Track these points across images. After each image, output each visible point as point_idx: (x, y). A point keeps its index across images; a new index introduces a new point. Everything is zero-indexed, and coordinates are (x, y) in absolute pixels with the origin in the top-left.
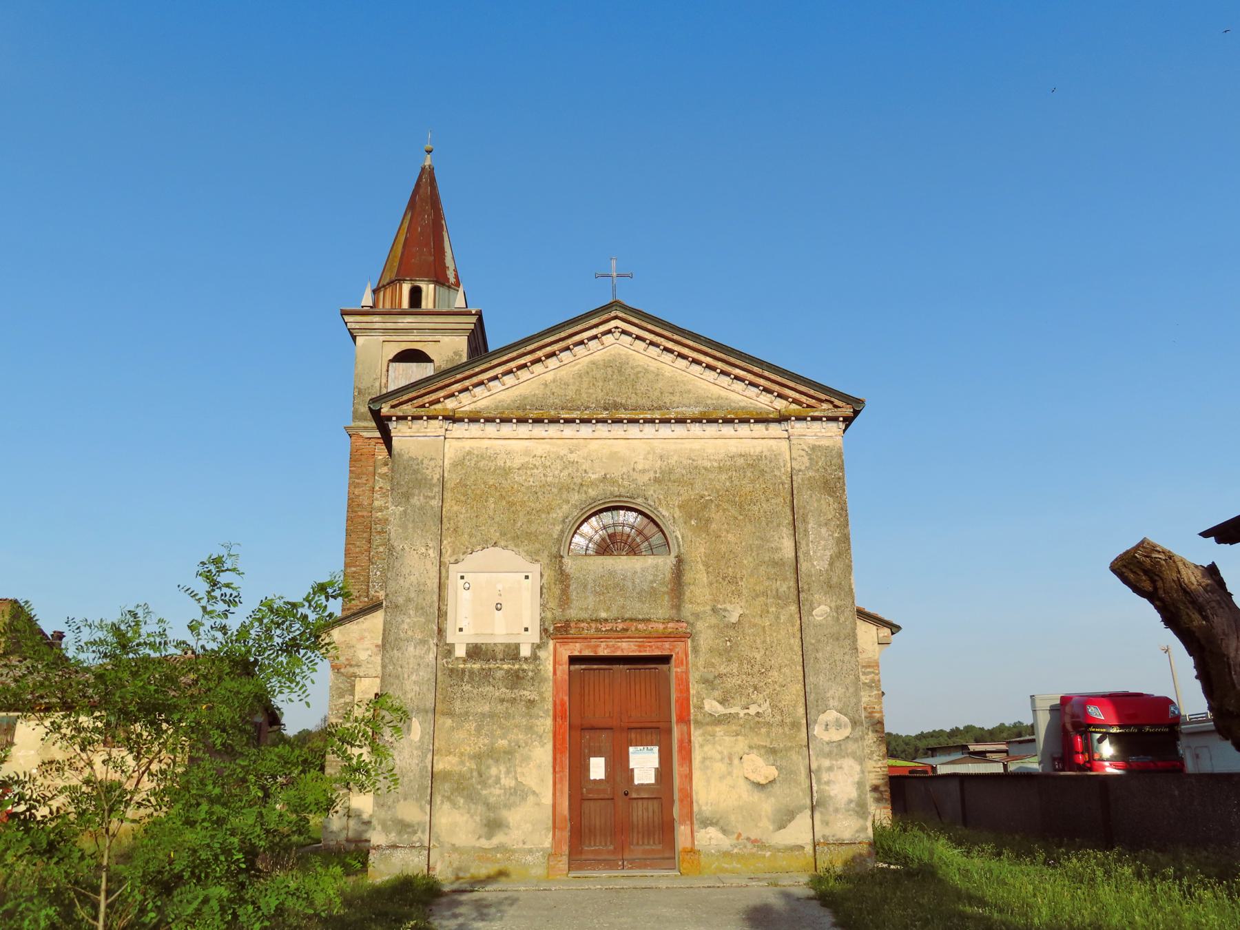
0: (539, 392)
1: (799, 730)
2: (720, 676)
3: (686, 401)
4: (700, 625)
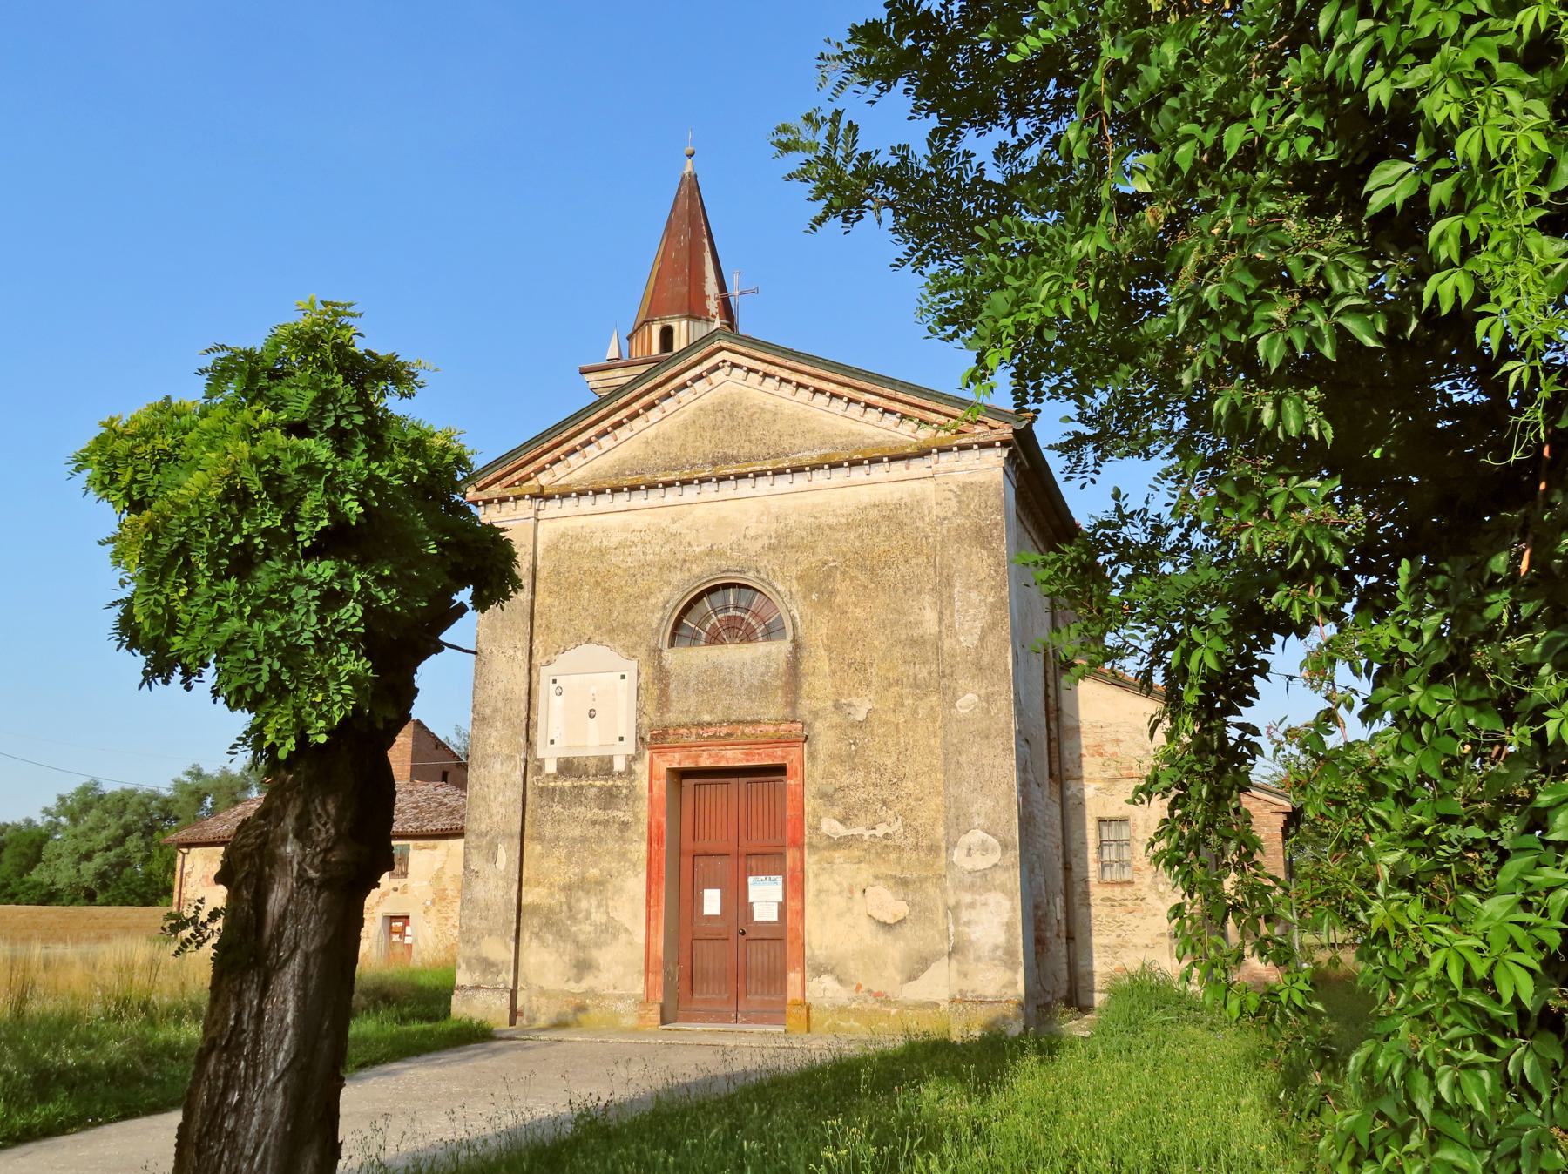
0: (640, 453)
1: (938, 855)
2: (841, 788)
3: (809, 443)
4: (819, 726)
